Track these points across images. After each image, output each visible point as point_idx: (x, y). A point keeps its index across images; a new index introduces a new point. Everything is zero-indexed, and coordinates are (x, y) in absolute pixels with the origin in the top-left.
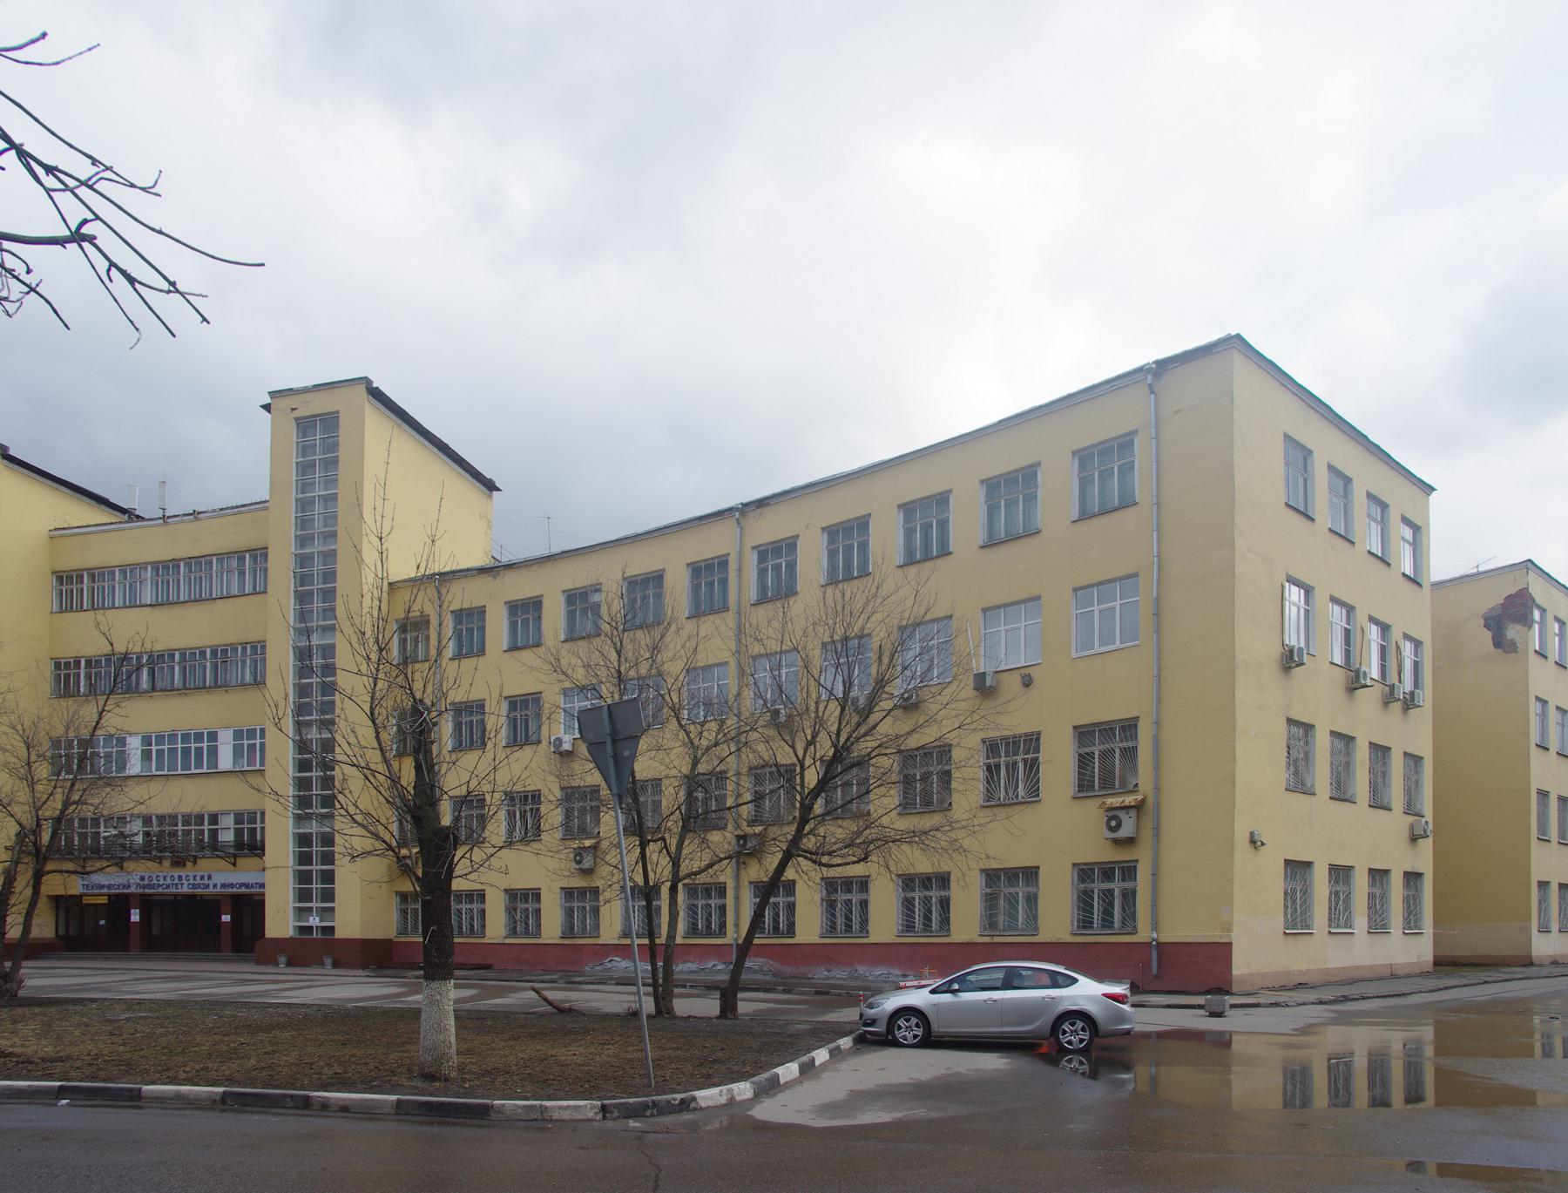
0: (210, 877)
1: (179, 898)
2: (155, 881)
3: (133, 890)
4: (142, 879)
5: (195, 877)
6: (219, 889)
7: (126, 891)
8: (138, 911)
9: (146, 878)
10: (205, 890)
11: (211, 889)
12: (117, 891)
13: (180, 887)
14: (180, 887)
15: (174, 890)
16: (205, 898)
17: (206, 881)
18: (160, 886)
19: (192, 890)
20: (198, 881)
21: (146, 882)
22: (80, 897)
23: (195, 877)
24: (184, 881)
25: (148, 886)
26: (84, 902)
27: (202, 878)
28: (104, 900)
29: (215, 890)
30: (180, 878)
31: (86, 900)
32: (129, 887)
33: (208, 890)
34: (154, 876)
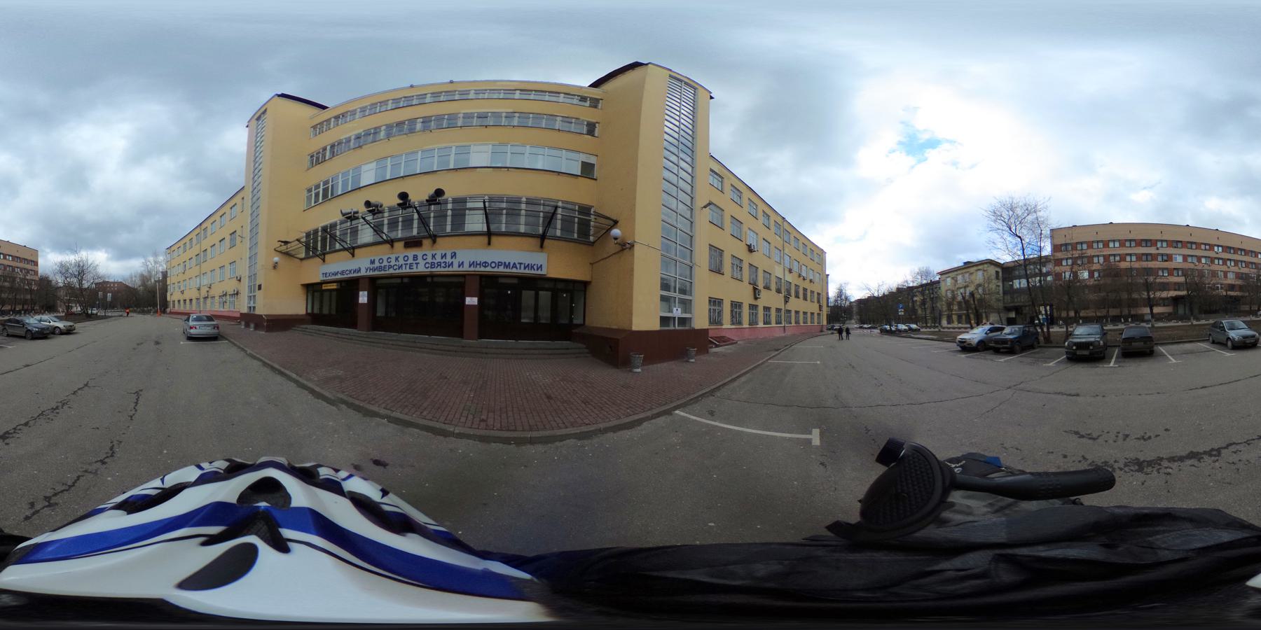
0: (454, 255)
1: (406, 280)
2: (385, 263)
3: (363, 273)
4: (373, 262)
5: (433, 256)
6: (466, 268)
7: (355, 275)
8: (366, 293)
9: (377, 262)
10: (447, 269)
11: (455, 268)
12: (349, 276)
13: (415, 266)
14: (415, 266)
15: (408, 270)
16: (436, 279)
17: (449, 260)
18: (390, 267)
19: (429, 270)
20: (438, 259)
21: (377, 264)
22: (321, 284)
23: (433, 256)
24: (420, 260)
25: (380, 269)
26: (323, 288)
27: (444, 256)
28: (334, 286)
29: (461, 269)
30: (415, 257)
31: (325, 287)
32: (359, 270)
33: (450, 269)
34: (385, 258)
